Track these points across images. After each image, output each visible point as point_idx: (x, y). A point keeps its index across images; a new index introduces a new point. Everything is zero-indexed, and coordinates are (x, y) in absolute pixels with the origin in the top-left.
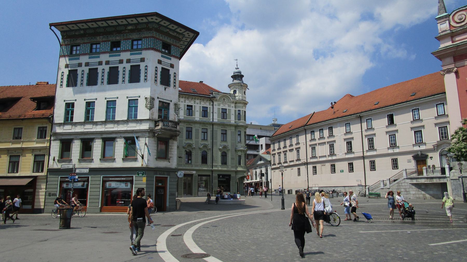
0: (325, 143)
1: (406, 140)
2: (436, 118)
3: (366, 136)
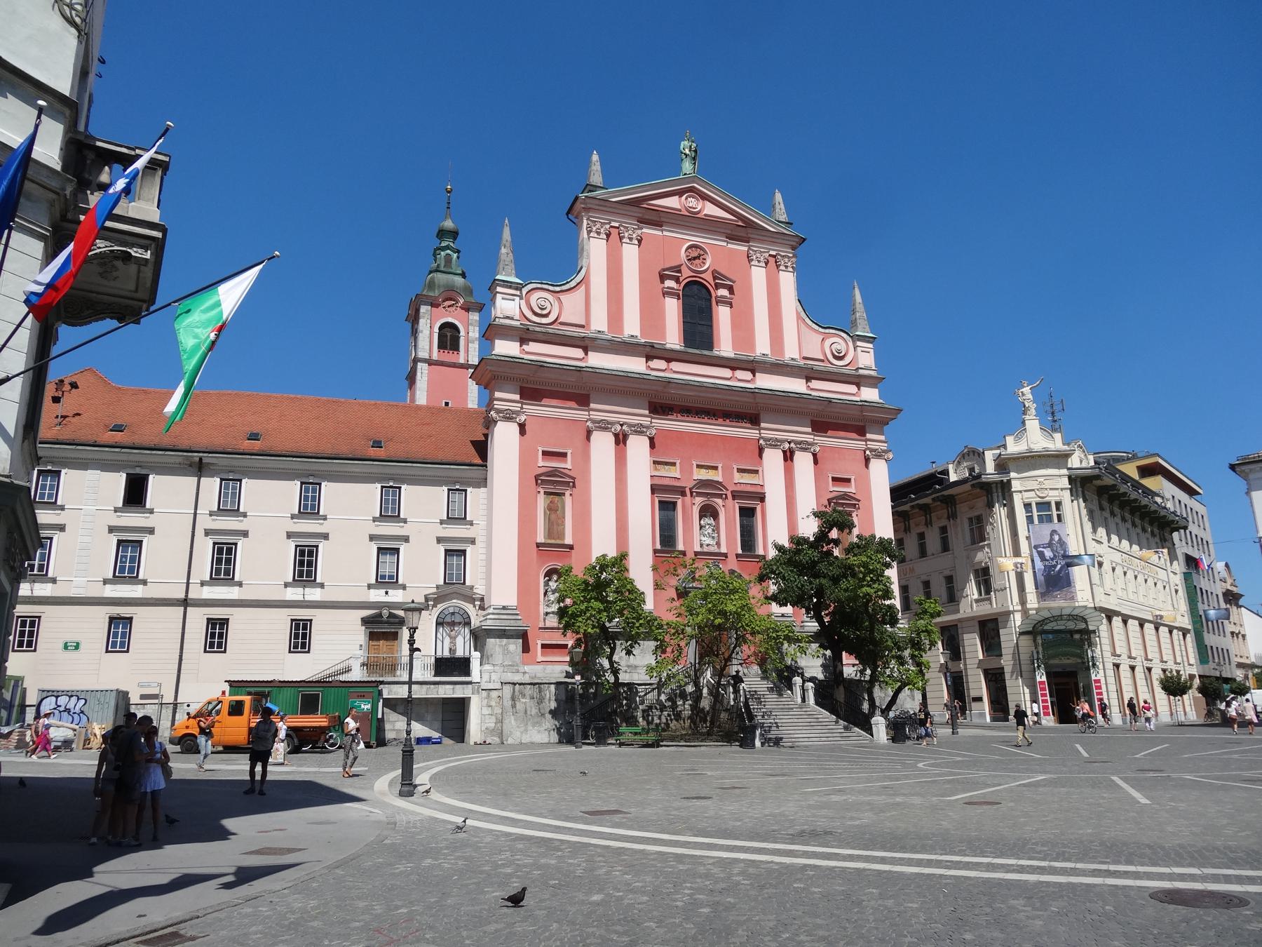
3: (208, 533)
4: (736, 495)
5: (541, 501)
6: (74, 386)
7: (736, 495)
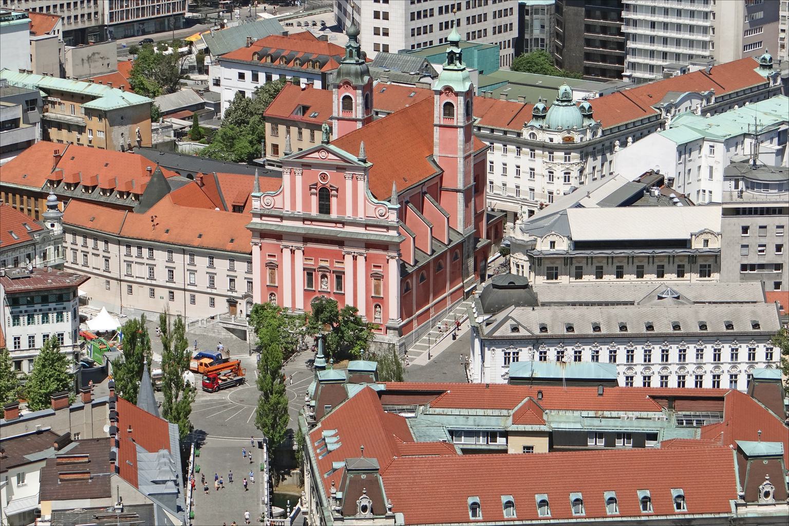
0: (144, 264)
1: (222, 285)
2: (246, 272)
4: (334, 272)
5: (268, 271)
6: (156, 216)
7: (334, 272)
